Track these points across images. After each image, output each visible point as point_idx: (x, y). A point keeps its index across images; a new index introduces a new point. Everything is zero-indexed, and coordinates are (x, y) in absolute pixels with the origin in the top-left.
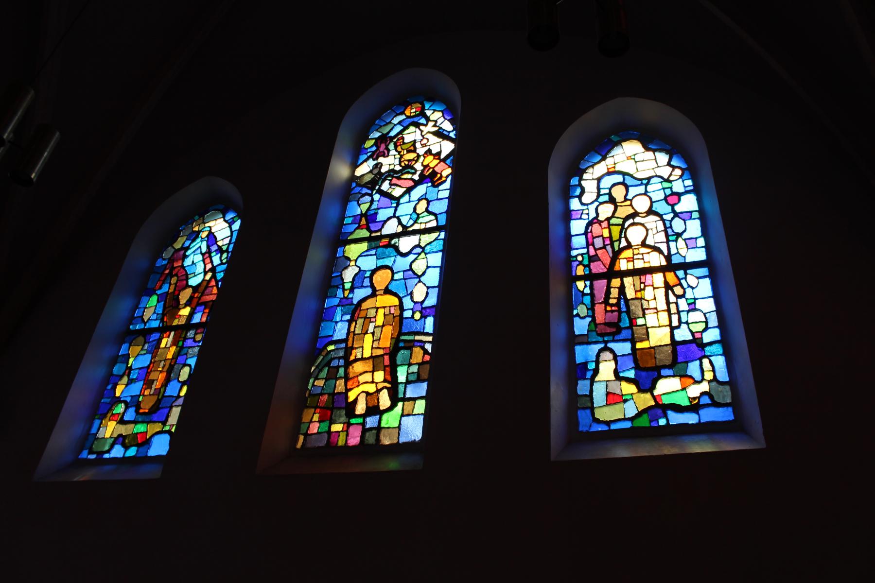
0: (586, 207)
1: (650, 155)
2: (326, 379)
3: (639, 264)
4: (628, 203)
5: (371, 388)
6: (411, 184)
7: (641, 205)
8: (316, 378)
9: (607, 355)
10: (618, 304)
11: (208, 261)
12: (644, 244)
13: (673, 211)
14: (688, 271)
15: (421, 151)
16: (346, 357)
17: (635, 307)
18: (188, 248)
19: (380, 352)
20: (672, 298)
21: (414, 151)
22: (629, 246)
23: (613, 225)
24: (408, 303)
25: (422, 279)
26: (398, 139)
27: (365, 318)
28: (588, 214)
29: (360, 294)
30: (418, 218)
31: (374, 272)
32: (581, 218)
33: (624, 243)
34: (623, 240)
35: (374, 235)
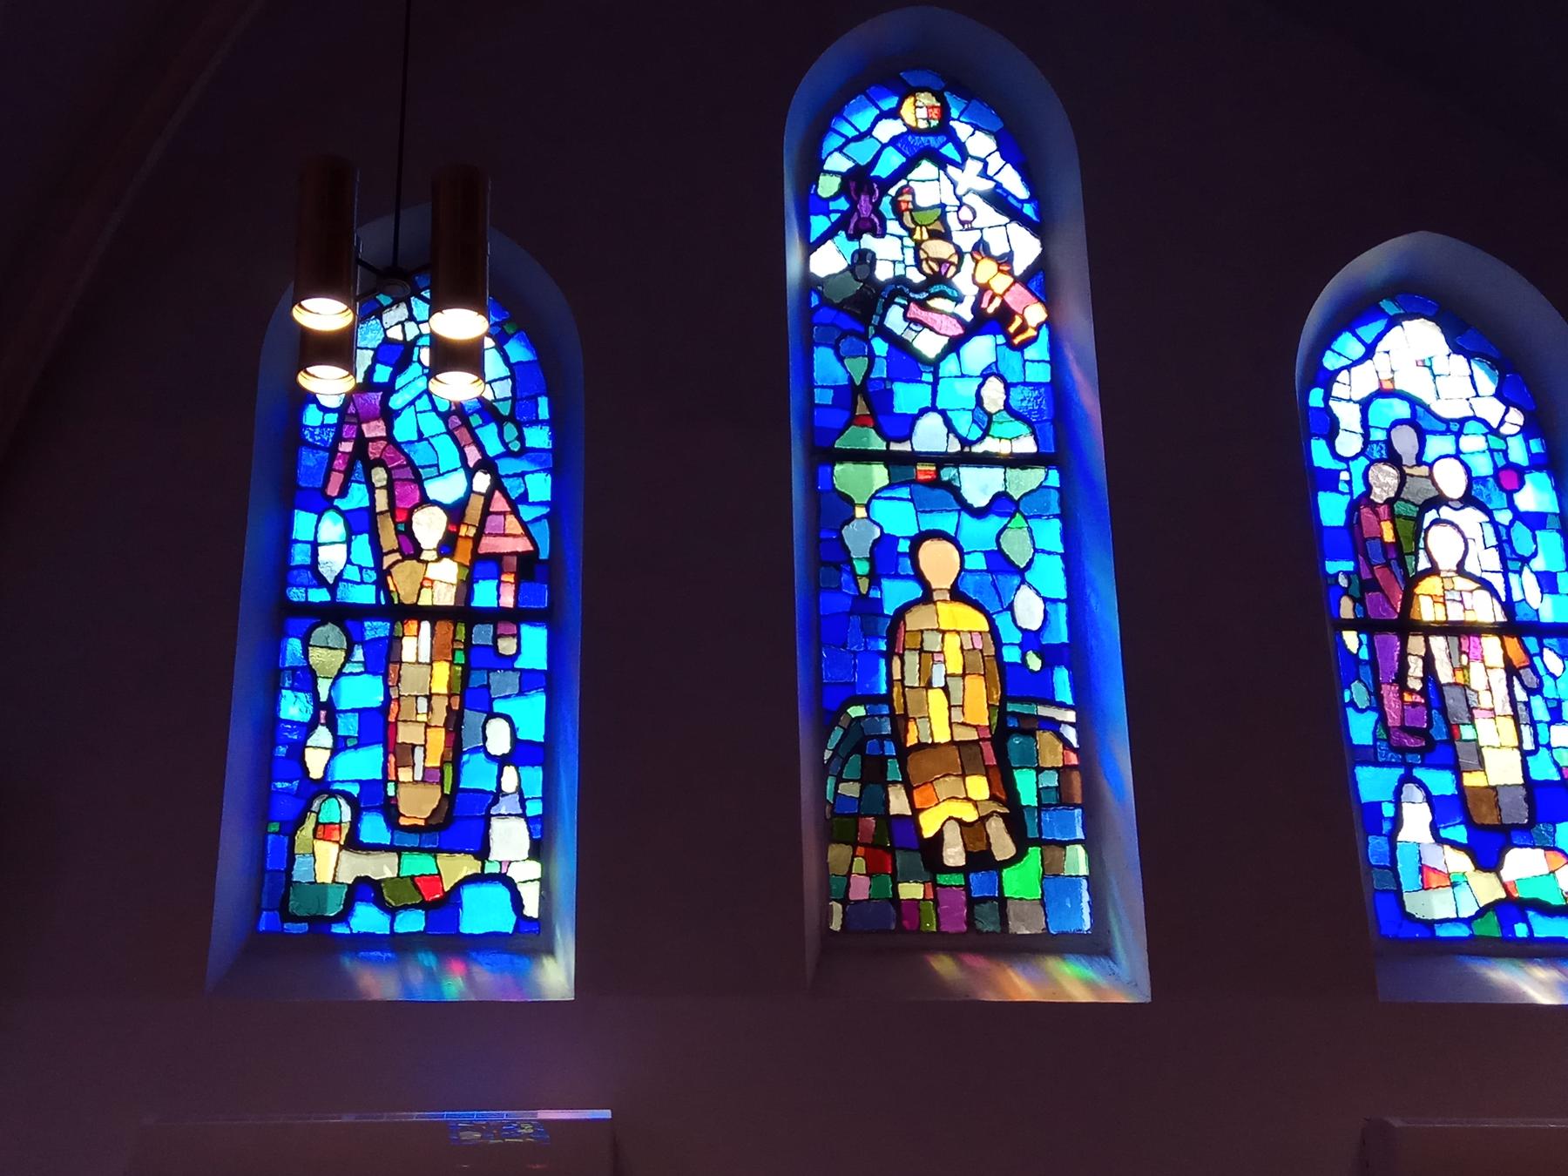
0: (1343, 466)
1: (1460, 360)
2: (864, 782)
3: (1456, 614)
4: (1424, 470)
5: (970, 815)
6: (958, 331)
7: (1451, 480)
8: (839, 780)
9: (1411, 790)
10: (1422, 693)
11: (463, 434)
12: (1460, 570)
13: (1511, 505)
14: (1546, 641)
15: (966, 240)
16: (898, 735)
17: (1452, 700)
18: (389, 389)
19: (973, 735)
20: (1521, 695)
21: (946, 236)
22: (1434, 570)
23: (1400, 516)
24: (1003, 621)
25: (1028, 576)
26: (900, 192)
27: (921, 651)
28: (1349, 483)
29: (895, 593)
30: (990, 422)
31: (917, 541)
32: (1336, 490)
33: (1424, 564)
34: (1422, 554)
35: (895, 447)
